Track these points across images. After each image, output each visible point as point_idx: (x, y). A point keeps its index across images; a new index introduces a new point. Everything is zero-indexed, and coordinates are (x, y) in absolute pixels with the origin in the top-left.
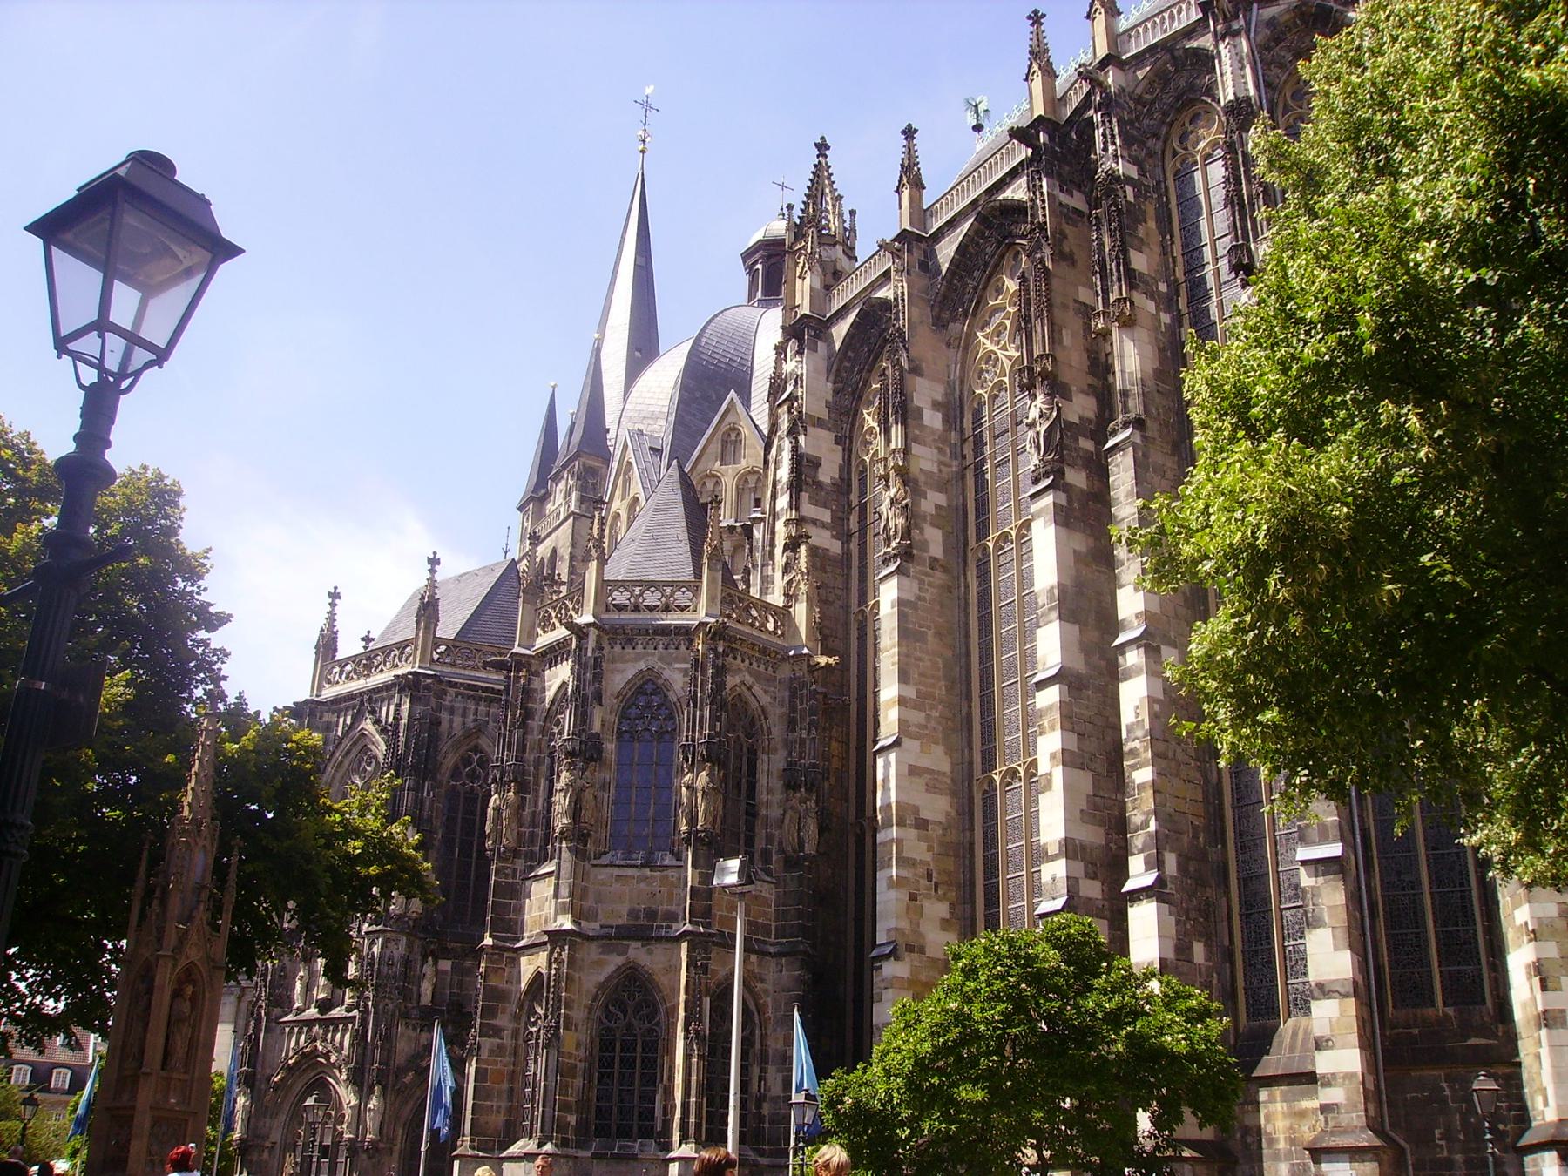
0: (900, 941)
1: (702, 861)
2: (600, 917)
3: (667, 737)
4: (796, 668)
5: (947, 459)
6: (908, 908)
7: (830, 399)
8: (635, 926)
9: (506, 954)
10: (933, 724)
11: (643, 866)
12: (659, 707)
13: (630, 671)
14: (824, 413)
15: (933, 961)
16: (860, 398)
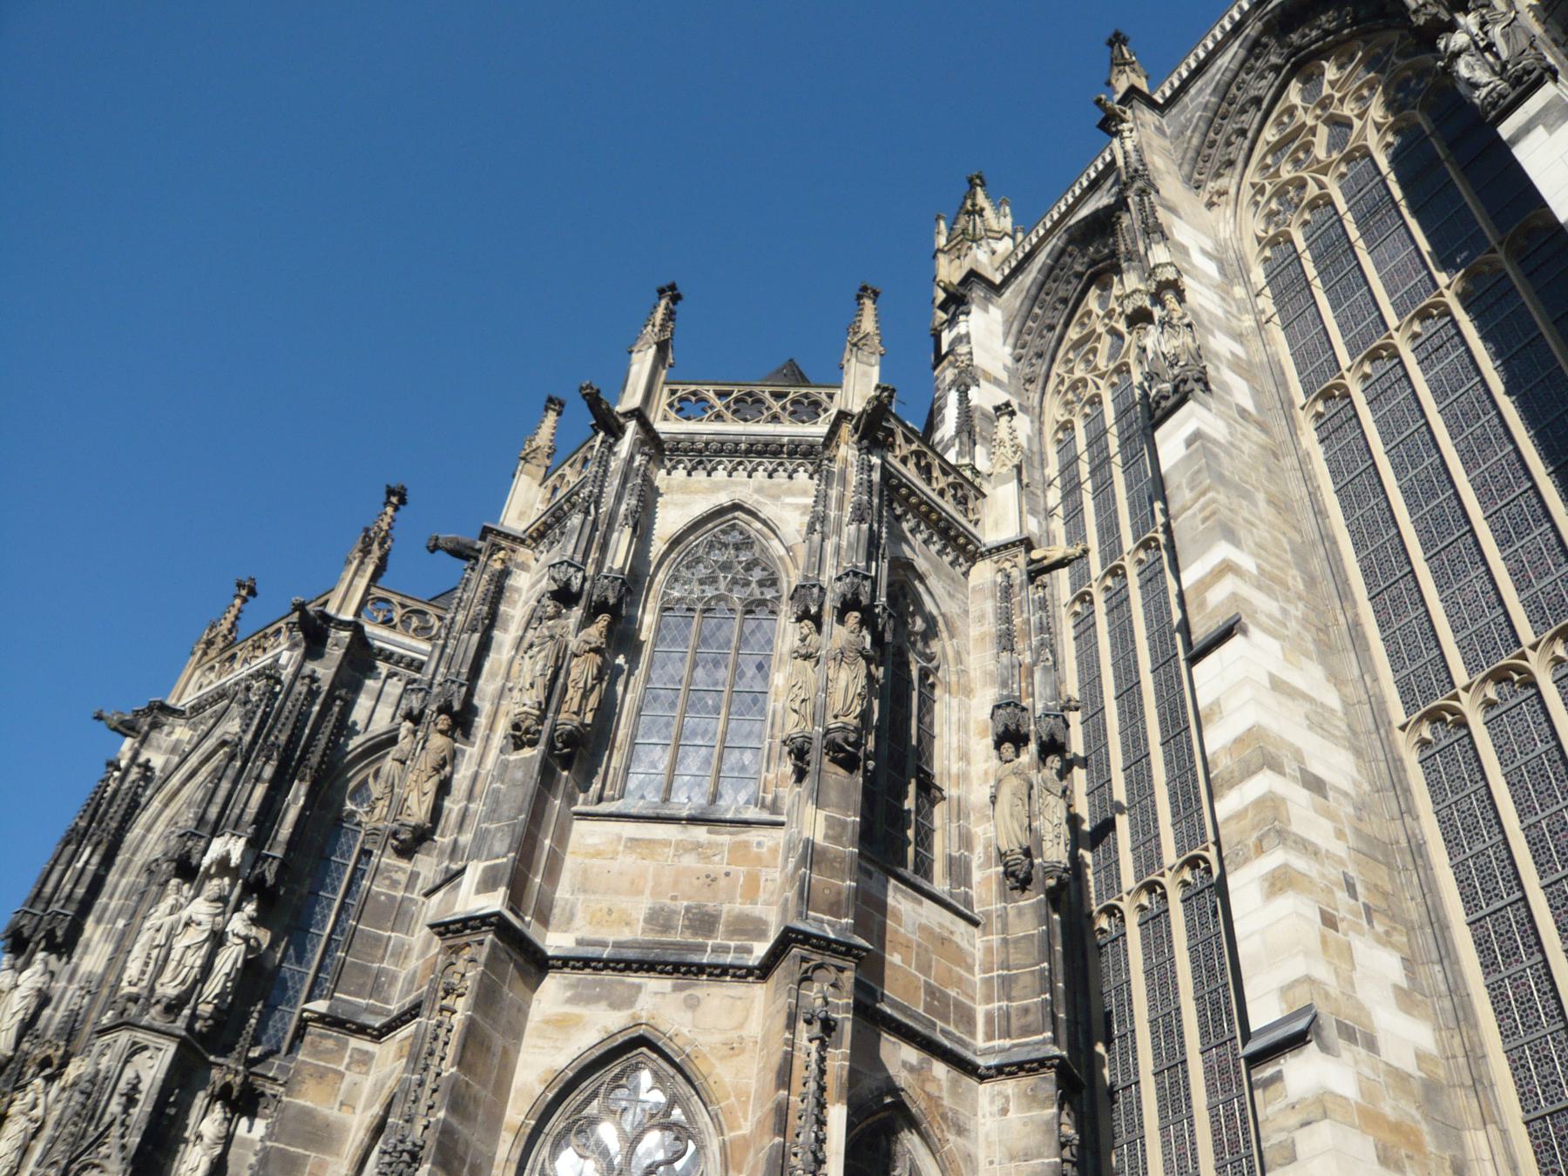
0: (1323, 1009)
1: (833, 795)
2: (579, 920)
3: (762, 613)
4: (1007, 565)
5: (1234, 310)
6: (1324, 942)
7: (1009, 361)
8: (661, 945)
9: (355, 1042)
10: (1294, 626)
11: (693, 820)
12: (749, 567)
13: (701, 506)
14: (1004, 376)
15: (1399, 1077)
16: (1053, 360)
